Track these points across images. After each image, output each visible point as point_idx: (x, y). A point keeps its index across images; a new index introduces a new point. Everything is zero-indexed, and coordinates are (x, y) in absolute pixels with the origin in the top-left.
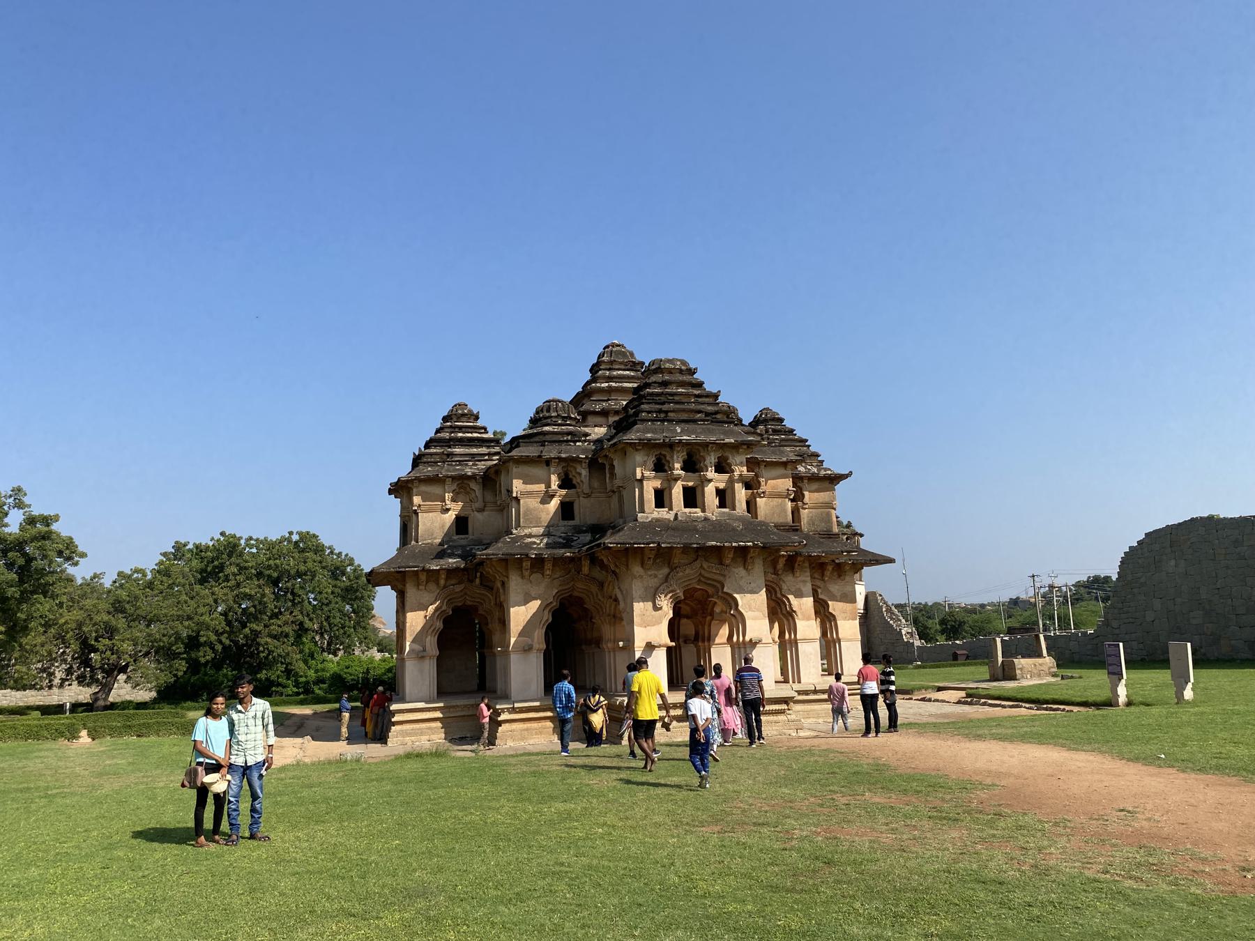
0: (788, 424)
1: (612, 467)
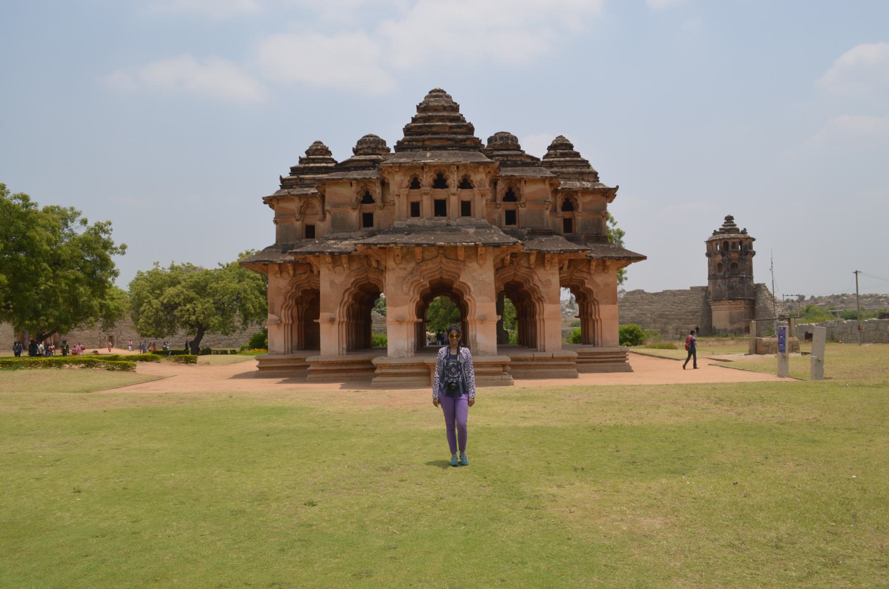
0: (575, 149)
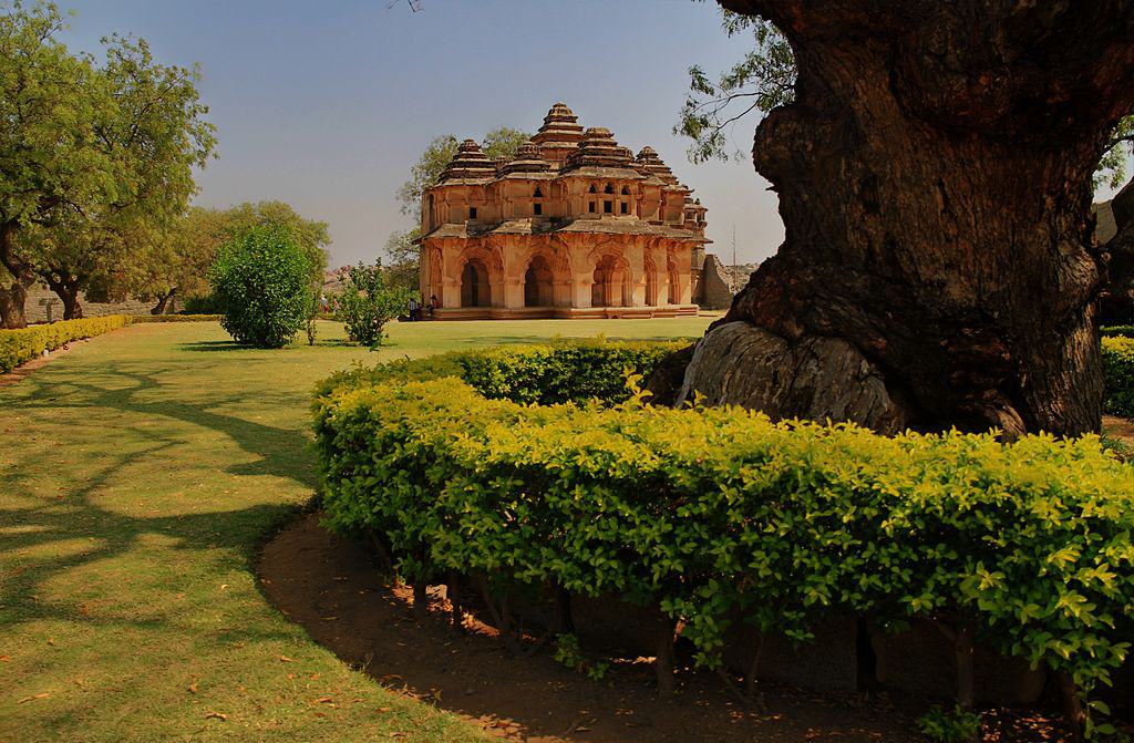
0: (660, 158)
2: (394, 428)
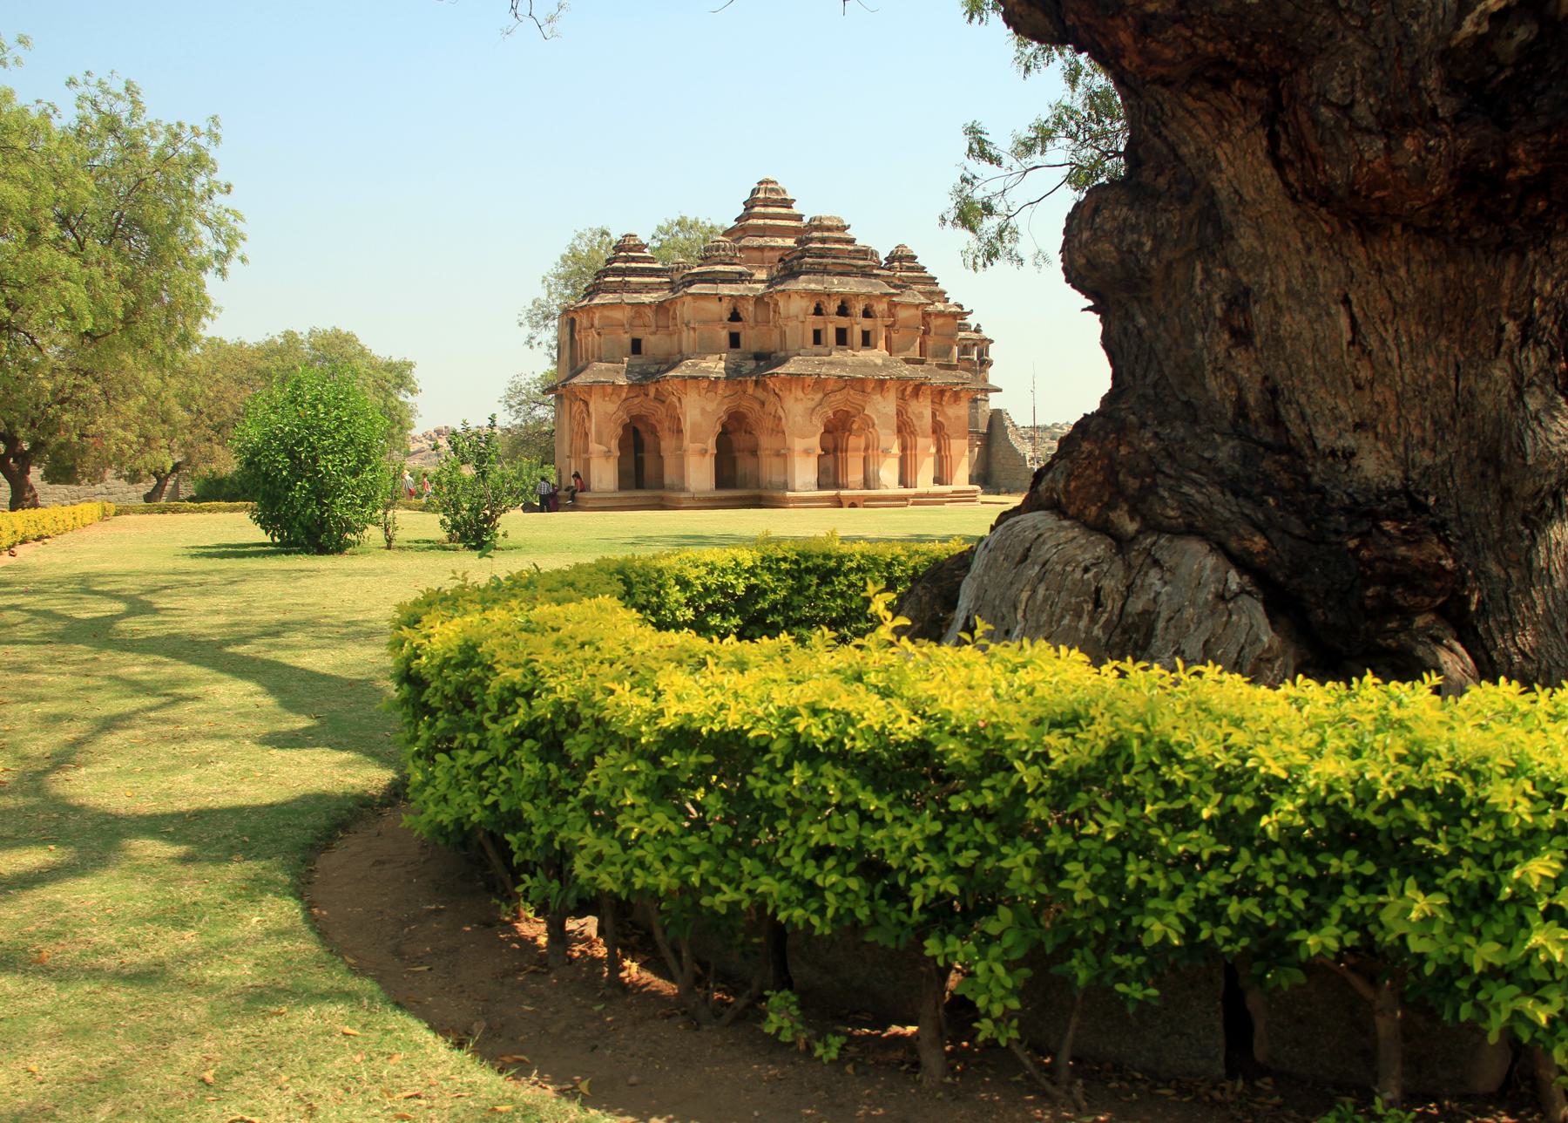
0: (921, 261)
1: (776, 304)
2: (516, 675)
